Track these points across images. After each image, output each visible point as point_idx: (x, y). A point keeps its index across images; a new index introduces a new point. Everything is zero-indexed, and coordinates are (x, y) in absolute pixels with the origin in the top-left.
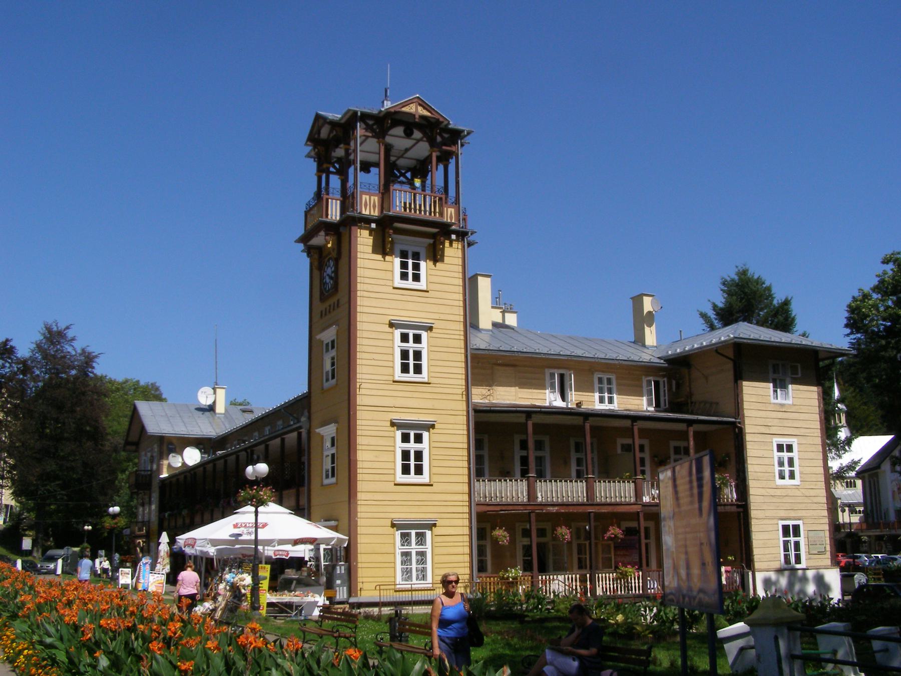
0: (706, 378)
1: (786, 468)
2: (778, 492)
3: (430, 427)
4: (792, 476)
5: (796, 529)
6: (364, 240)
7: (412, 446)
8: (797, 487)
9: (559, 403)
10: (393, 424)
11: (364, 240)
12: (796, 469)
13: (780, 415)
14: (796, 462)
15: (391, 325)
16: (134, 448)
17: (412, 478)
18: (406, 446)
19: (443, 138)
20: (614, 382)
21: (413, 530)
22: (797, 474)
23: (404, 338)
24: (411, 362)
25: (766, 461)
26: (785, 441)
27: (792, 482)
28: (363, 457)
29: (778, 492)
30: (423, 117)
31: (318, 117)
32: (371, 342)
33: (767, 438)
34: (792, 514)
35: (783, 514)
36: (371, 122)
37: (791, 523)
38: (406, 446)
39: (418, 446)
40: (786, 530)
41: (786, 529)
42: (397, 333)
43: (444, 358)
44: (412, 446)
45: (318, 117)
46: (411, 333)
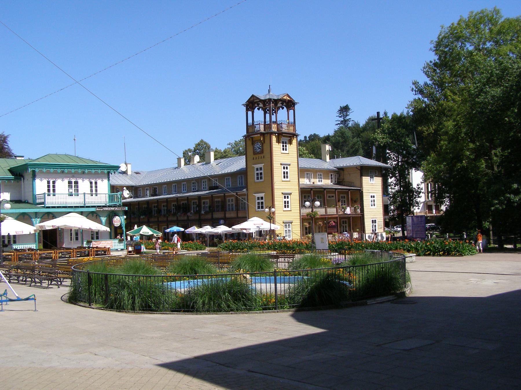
0: (350, 174)
2: (371, 210)
3: (290, 194)
5: (375, 221)
6: (274, 139)
8: (375, 209)
9: (309, 183)
10: (282, 194)
11: (274, 139)
12: (375, 203)
15: (281, 164)
19: (290, 104)
21: (287, 224)
26: (373, 195)
29: (371, 210)
30: (288, 100)
34: (374, 217)
35: (372, 217)
37: (374, 219)
40: (373, 222)
41: (373, 221)
42: (283, 166)
46: (285, 166)
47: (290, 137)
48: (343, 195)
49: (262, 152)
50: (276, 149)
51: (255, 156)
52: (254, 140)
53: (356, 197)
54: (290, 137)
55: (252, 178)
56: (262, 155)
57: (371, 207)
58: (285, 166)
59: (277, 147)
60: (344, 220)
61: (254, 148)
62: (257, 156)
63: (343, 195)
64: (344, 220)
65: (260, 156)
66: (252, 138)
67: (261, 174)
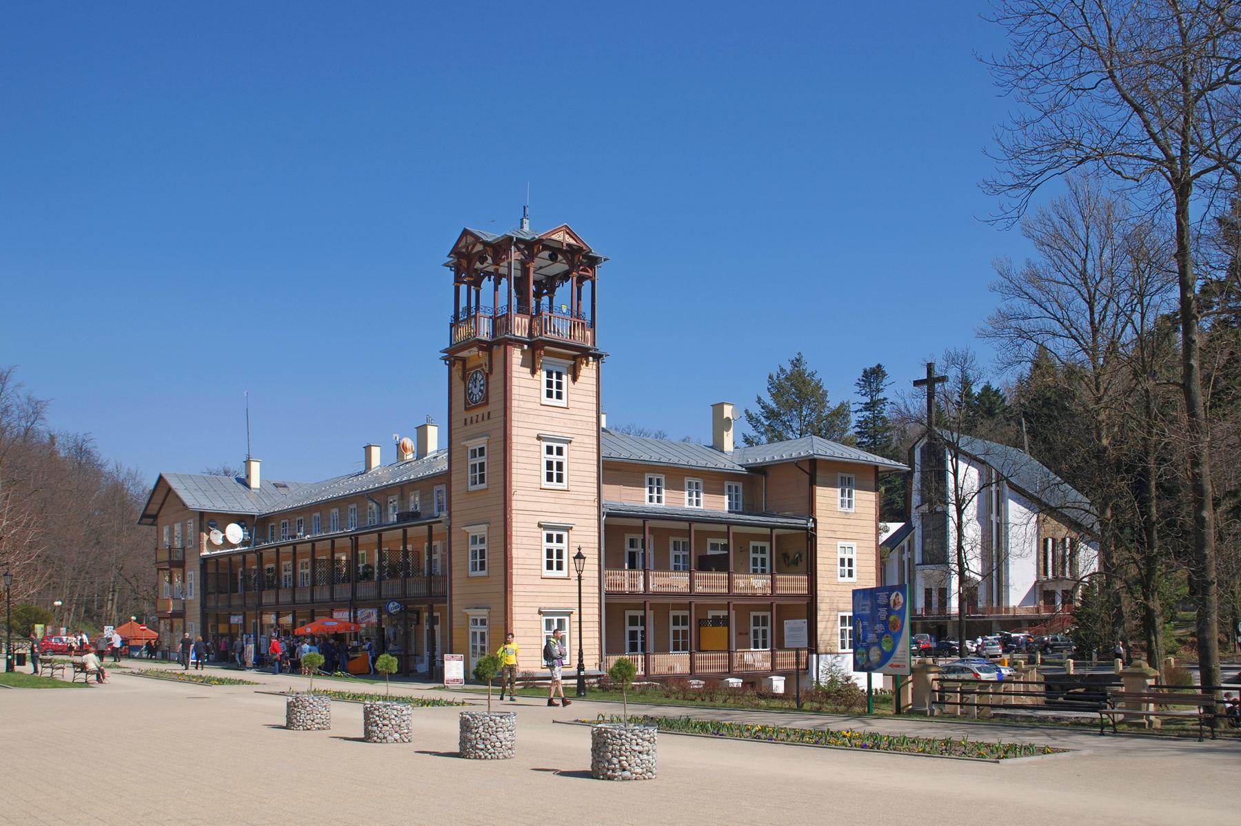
1: (847, 568)
2: (839, 588)
4: (850, 574)
6: (516, 355)
7: (555, 546)
10: (540, 526)
11: (516, 355)
12: (854, 568)
13: (845, 522)
14: (854, 563)
16: (151, 520)
17: (554, 573)
18: (550, 545)
19: (580, 261)
20: (701, 485)
22: (854, 573)
23: (549, 450)
24: (554, 472)
25: (831, 561)
27: (850, 580)
28: (517, 553)
30: (569, 245)
31: (466, 232)
32: (525, 454)
33: (833, 542)
36: (522, 246)
38: (550, 545)
39: (559, 546)
42: (544, 445)
43: (581, 465)
44: (555, 546)
45: (466, 232)
47: (574, 358)
48: (759, 544)
49: (486, 400)
50: (523, 391)
51: (469, 415)
52: (469, 366)
53: (799, 552)
54: (574, 358)
55: (463, 482)
56: (484, 410)
57: (841, 580)
58: (555, 445)
59: (526, 386)
60: (760, 614)
61: (466, 389)
62: (473, 413)
63: (759, 544)
64: (760, 614)
65: (480, 412)
66: (464, 360)
67: (482, 465)
